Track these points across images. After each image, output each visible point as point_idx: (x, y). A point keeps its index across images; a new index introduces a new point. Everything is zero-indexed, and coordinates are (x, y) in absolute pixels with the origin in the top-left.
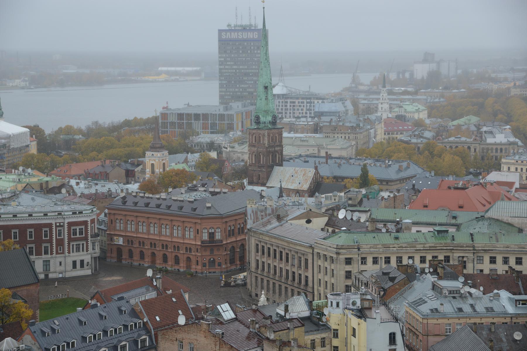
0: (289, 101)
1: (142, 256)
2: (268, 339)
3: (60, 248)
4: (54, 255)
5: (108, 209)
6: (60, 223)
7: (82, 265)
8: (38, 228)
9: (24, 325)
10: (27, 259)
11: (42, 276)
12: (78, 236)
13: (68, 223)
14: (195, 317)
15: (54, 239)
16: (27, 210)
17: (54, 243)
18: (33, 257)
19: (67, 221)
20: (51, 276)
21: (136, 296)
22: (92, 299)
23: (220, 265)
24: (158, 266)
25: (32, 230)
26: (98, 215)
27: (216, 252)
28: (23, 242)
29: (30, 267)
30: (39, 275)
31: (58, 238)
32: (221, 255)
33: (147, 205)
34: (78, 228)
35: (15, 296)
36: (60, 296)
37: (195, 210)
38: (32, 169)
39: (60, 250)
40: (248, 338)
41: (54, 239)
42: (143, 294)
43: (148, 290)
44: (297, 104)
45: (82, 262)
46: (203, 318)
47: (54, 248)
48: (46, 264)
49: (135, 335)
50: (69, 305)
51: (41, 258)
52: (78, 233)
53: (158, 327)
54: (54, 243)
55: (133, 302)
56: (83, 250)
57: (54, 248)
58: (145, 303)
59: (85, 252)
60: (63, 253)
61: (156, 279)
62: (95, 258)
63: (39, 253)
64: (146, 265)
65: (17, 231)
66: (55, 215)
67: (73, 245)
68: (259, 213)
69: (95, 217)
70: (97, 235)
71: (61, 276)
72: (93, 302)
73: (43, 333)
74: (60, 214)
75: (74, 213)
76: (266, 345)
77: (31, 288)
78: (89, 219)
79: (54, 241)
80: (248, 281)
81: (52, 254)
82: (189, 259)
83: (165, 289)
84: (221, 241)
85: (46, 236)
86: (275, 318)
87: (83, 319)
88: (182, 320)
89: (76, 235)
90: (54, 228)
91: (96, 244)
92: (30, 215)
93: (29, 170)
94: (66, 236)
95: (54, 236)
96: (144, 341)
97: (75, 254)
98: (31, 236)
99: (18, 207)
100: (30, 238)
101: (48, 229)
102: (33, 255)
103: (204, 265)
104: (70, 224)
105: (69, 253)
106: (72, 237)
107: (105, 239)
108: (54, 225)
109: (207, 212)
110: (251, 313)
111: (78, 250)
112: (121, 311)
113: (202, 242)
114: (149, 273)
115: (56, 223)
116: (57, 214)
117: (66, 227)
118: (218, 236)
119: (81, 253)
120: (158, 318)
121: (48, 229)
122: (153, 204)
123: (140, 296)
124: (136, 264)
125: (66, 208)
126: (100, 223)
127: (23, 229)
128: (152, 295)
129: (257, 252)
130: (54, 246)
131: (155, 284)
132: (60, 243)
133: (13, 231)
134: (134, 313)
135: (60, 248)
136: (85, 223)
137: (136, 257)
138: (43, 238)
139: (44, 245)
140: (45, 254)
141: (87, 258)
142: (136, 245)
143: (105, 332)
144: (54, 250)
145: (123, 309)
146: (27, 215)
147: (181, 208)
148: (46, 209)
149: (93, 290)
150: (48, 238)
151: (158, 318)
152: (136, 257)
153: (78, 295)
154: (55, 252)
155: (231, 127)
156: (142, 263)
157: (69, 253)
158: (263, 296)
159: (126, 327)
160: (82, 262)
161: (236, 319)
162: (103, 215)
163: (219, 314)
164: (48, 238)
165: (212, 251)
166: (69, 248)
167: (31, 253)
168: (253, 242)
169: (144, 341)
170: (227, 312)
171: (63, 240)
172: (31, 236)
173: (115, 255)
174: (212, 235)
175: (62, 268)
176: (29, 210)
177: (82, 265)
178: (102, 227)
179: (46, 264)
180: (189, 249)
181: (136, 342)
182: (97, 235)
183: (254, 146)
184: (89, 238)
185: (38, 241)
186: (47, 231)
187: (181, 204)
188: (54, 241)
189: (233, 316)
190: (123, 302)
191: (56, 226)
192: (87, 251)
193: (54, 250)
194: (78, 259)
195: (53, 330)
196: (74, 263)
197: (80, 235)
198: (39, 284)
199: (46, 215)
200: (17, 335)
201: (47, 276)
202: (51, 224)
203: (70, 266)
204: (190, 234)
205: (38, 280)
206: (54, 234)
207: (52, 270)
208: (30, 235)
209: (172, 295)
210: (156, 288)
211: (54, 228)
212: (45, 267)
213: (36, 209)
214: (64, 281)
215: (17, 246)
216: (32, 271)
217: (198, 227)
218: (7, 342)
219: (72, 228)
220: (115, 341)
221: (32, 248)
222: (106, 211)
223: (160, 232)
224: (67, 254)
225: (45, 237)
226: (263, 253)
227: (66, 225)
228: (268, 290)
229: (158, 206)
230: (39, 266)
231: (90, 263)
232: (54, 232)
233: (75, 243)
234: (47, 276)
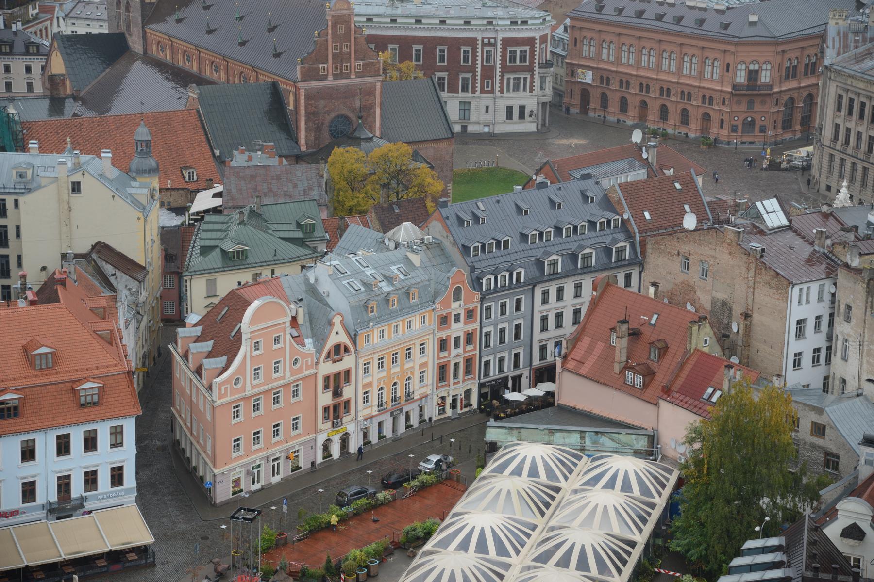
1: (624, 105)
2: (847, 266)
3: (488, 82)
4: (478, 94)
5: (572, 18)
6: (489, 39)
7: (522, 115)
8: (454, 44)
9: (430, 204)
10: (435, 97)
11: (457, 128)
12: (518, 63)
13: (503, 40)
14: (714, 220)
15: (479, 66)
16: (437, 13)
17: (479, 74)
18: (444, 95)
19: (501, 36)
20: (471, 129)
21: (611, 174)
22: (537, 173)
23: (763, 130)
24: (652, 126)
25: (445, 48)
26: (554, 28)
27: (758, 107)
28: (429, 68)
29: (440, 110)
31: (485, 64)
32: (767, 113)
33: (640, 14)
34: (518, 49)
35: (416, 156)
36: (485, 164)
37: (726, 26)
39: (488, 87)
40: (810, 261)
41: (479, 66)
42: (623, 171)
43: (632, 167)
45: (522, 109)
46: (728, 222)
47: (479, 81)
48: (465, 107)
49: (608, 240)
50: (501, 179)
51: (457, 97)
52: (519, 57)
53: (647, 230)
54: (479, 74)
55: (606, 183)
56: (525, 90)
57: (479, 81)
58: (628, 188)
59: (528, 93)
60: (492, 92)
61: (648, 148)
62: (544, 104)
63: (453, 89)
64: (630, 122)
65: (421, 47)
66: (483, 25)
67: (509, 79)
68: (851, 36)
69: (548, 31)
70: (548, 65)
71: (486, 130)
72: (540, 179)
73: (460, 221)
74: (490, 23)
75: (514, 23)
76: (842, 275)
77: (443, 145)
78: (537, 35)
79: (479, 70)
80: (815, 162)
81: (474, 91)
82: (706, 117)
83: (662, 167)
84: (770, 87)
85: (466, 60)
86: (863, 231)
87: (524, 206)
88: (690, 222)
89: (515, 61)
90: (479, 46)
91: (548, 80)
92: (443, 22)
94: (499, 62)
95: (479, 62)
96: (621, 251)
97: (512, 94)
98: (442, 59)
99: (424, 7)
100: (440, 61)
101: (469, 48)
102: (444, 90)
103: (734, 129)
104: (507, 42)
105: (502, 91)
106: (508, 64)
107: (562, 72)
108: (480, 42)
109: (749, 32)
110: (818, 218)
111: (516, 88)
112: (585, 198)
113: (735, 87)
114: (637, 136)
115: (483, 39)
116: (485, 22)
117: (499, 46)
118: (765, 78)
119: (522, 93)
120: (647, 215)
122: (650, 14)
123: (617, 176)
124: (612, 119)
125: (500, 12)
126: (556, 43)
127: (430, 44)
128: (639, 175)
129: (839, 109)
130: (479, 77)
131: (645, 156)
132: (488, 73)
133: (415, 47)
134: (608, 203)
135: (488, 82)
136: (530, 41)
137: (614, 106)
138: (462, 64)
139: (462, 75)
140: (463, 91)
141: (531, 104)
142: (615, 86)
143: (558, 230)
144: (478, 85)
145: (589, 194)
146: (438, 22)
147: (701, 22)
148: (469, 13)
149: (540, 158)
150: (470, 64)
151: (647, 215)
152: (614, 106)
153: (513, 164)
154: (478, 89)
156: (622, 118)
157: (502, 91)
158: (844, 190)
159: (592, 224)
160: (522, 109)
161: (789, 227)
162: (561, 30)
163: (759, 216)
164: (470, 64)
165: (751, 103)
166: (502, 83)
168: (833, 90)
169: (621, 251)
170: (772, 213)
171: (492, 69)
173: (577, 100)
174: (753, 75)
175: (489, 117)
176: (441, 13)
177: (522, 115)
178: (559, 51)
179: (465, 107)
180: (708, 99)
181: (608, 251)
182: (548, 65)
184: (536, 69)
185: (454, 69)
186: (468, 52)
187: (703, 15)
188: (479, 70)
189: (784, 222)
190: (590, 183)
191: (483, 44)
193: (478, 85)
194: (516, 104)
195: (476, 218)
196: (510, 109)
197: (521, 61)
198: (453, 140)
199: (467, 23)
200: (421, 218)
201: (464, 128)
202: (476, 40)
203: (502, 115)
204: (713, 72)
205: (452, 133)
206: (479, 58)
207: (473, 118)
208: (440, 56)
209: (674, 178)
210: (646, 163)
211: (479, 46)
212: (462, 112)
213: (452, 12)
214: (492, 138)
215: (421, 74)
216: (443, 118)
217: (730, 59)
218: (406, 229)
219: (510, 49)
220: (573, 247)
221: (444, 78)
222: (568, 22)
223: (659, 65)
224: (498, 94)
225: (464, 62)
226: (850, 113)
227: (499, 42)
228: (852, 181)
229: (660, 17)
230: (453, 110)
231: (535, 113)
232: (479, 54)
233: (512, 76)
234: (464, 128)
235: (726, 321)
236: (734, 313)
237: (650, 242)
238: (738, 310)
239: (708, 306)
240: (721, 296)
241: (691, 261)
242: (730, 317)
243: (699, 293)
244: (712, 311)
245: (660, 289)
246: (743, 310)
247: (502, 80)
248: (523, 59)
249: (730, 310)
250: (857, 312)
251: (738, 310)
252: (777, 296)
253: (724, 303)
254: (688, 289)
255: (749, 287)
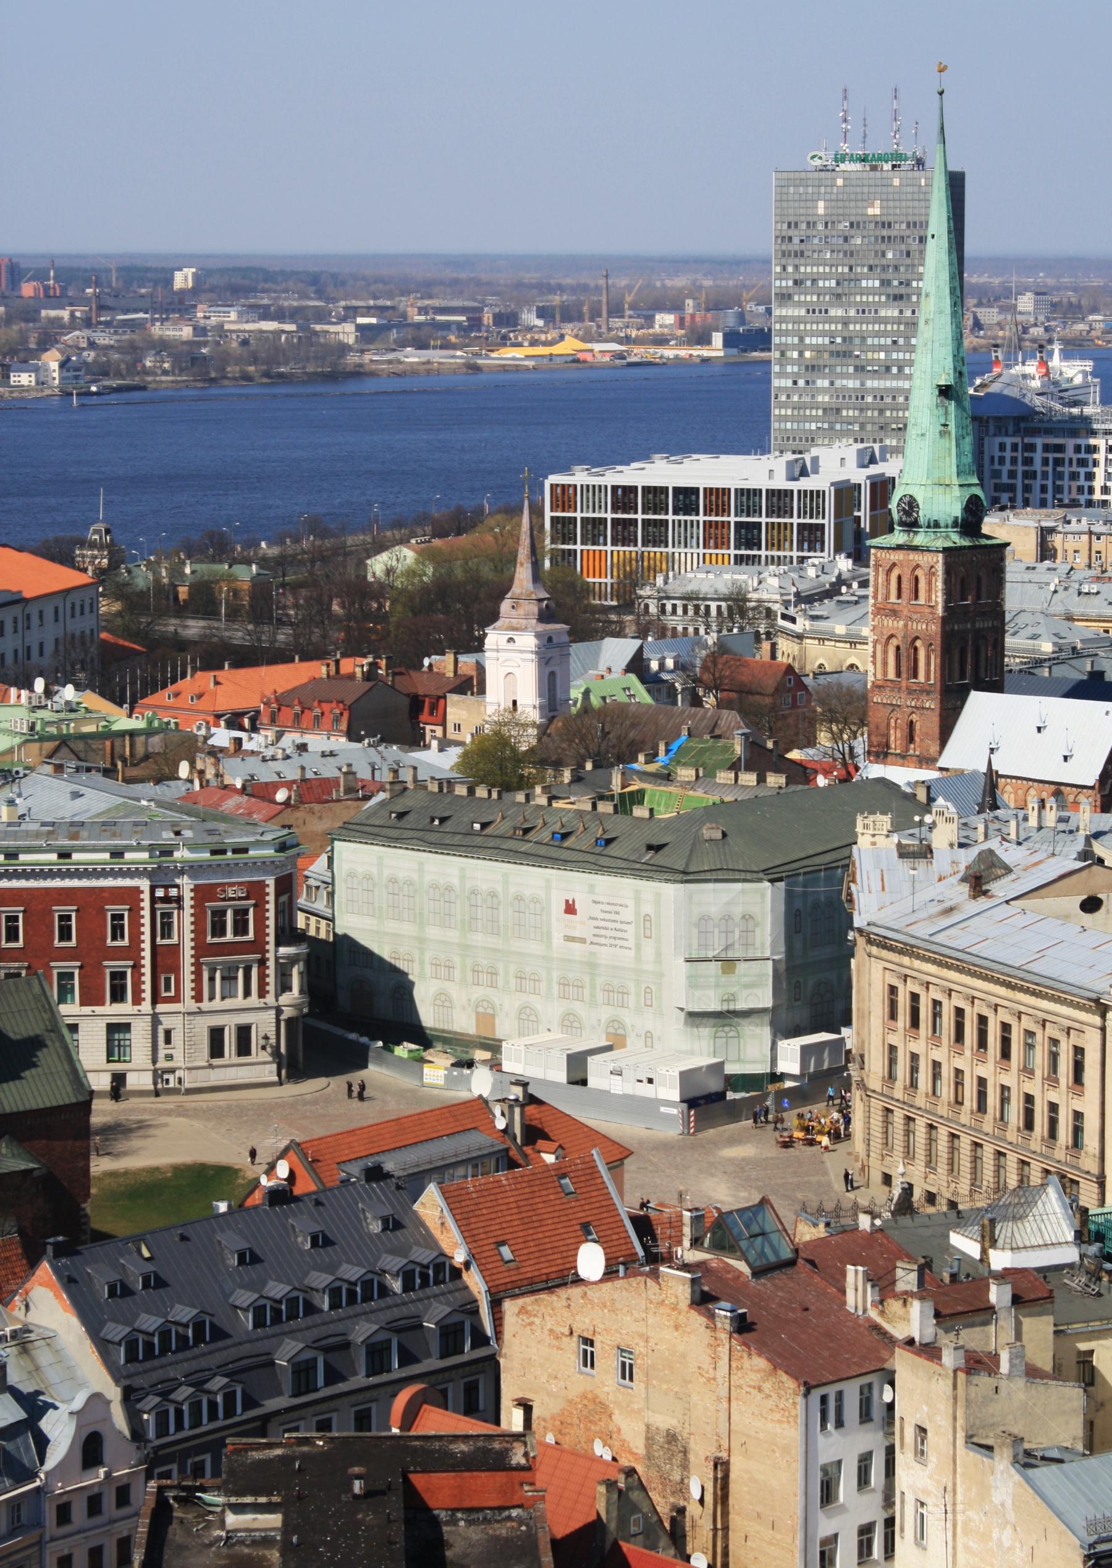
0: (1039, 442)
7: (244, 1049)
12: (229, 936)
17: (147, 962)
18: (70, 1010)
25: (71, 909)
30: (90, 1076)
38: (78, 687)
41: (147, 946)
44: (1070, 453)
56: (247, 993)
57: (147, 978)
59: (254, 1000)
63: (91, 998)
67: (212, 972)
79: (147, 954)
81: (137, 1000)
85: (117, 932)
89: (223, 933)
91: (295, 972)
93: (69, 692)
94: (188, 936)
95: (146, 937)
101: (123, 909)
106: (209, 939)
108: (146, 896)
117: (188, 903)
121: (123, 909)
135: (168, 980)
141: (264, 1024)
150: (126, 942)
154: (147, 995)
155: (811, 537)
157: (198, 998)
166: (198, 980)
167: (65, 993)
171: (175, 949)
172: (65, 934)
177: (244, 1049)
183: (894, 613)
184: (271, 947)
185: (91, 954)
191: (154, 900)
192: (262, 994)
193: (147, 987)
194: (230, 1023)
197: (236, 933)
201: (119, 1079)
208: (61, 928)
211: (146, 904)
231: (273, 1041)
234: (119, 1079)
235: (676, 1476)
236: (692, 1457)
237: (510, 1307)
238: (701, 1452)
239: (638, 1445)
240: (664, 1421)
241: (597, 1349)
242: (685, 1466)
243: (617, 1417)
244: (649, 1457)
245: (536, 1413)
246: (712, 1451)
247: (198, 974)
248: (241, 927)
249: (685, 1452)
250: (938, 1442)
251: (701, 1452)
252: (778, 1416)
253: (671, 1437)
254: (595, 1410)
255: (719, 1399)
